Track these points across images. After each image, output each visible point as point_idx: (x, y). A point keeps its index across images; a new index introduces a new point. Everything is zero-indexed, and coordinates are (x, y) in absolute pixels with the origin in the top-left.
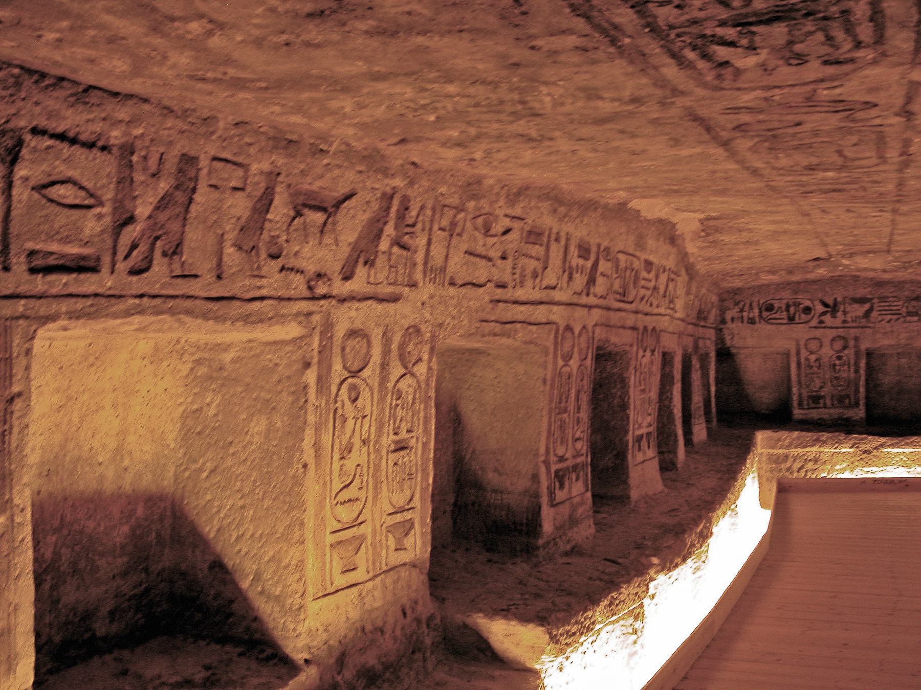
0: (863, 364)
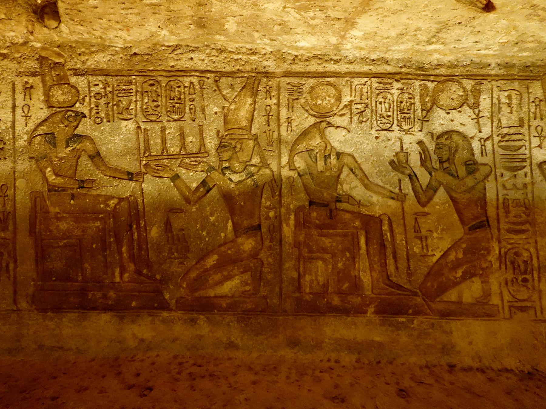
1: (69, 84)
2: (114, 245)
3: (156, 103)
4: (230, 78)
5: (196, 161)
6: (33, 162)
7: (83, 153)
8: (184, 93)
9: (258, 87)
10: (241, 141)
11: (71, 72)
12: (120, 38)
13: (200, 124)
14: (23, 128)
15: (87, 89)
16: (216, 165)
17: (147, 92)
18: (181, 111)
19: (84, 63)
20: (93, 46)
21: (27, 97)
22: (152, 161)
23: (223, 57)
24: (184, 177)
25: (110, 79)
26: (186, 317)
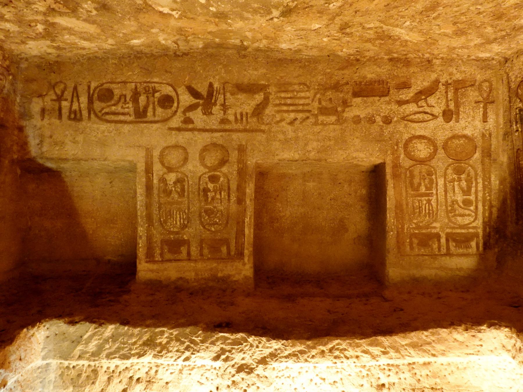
0: (250, 189)
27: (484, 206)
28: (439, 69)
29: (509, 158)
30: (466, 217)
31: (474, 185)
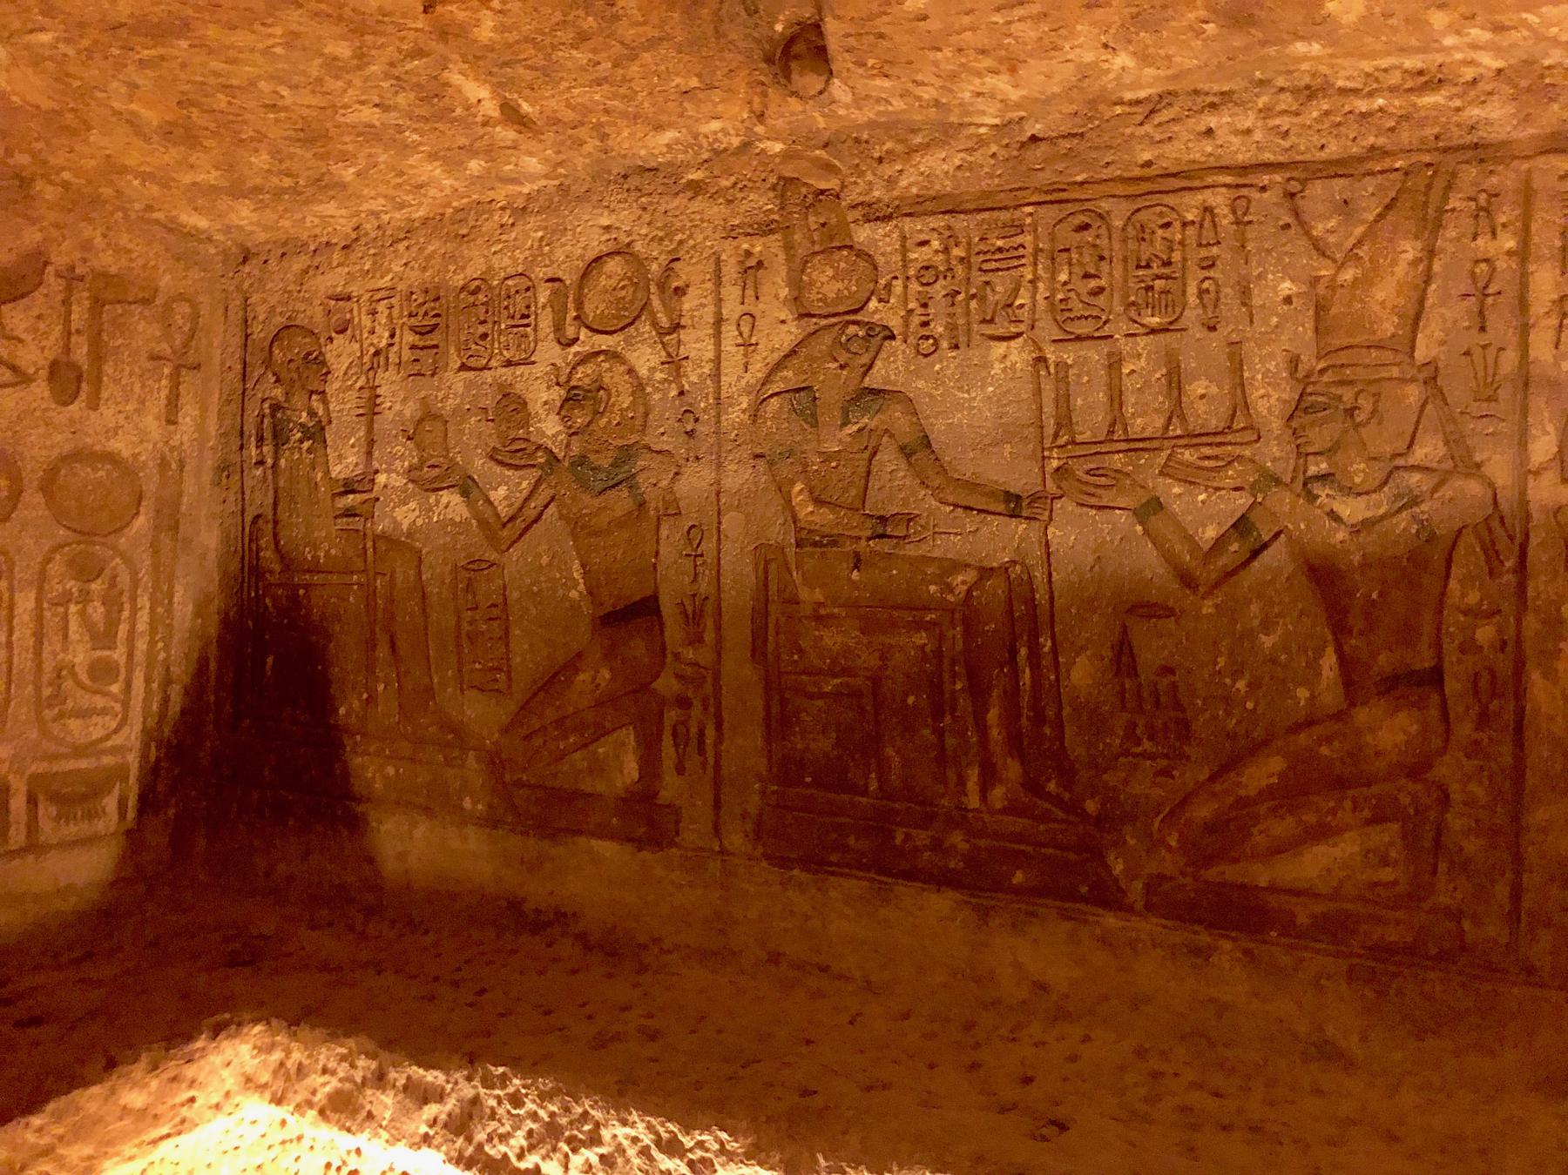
1: (851, 247)
2: (964, 703)
3: (1093, 283)
4: (1342, 182)
5: (1216, 458)
6: (762, 465)
7: (885, 439)
8: (1182, 243)
9: (1445, 199)
10: (1373, 389)
11: (857, 214)
12: (990, 96)
13: (1234, 337)
14: (740, 378)
15: (897, 258)
16: (1285, 471)
17: (1067, 250)
18: (1171, 302)
19: (891, 182)
20: (914, 131)
21: (750, 292)
22: (1081, 460)
23: (1315, 114)
24: (1176, 507)
25: (960, 223)
26: (1178, 937)
27: (148, 681)
28: (52, 216)
29: (226, 539)
30: (95, 719)
31: (126, 614)
